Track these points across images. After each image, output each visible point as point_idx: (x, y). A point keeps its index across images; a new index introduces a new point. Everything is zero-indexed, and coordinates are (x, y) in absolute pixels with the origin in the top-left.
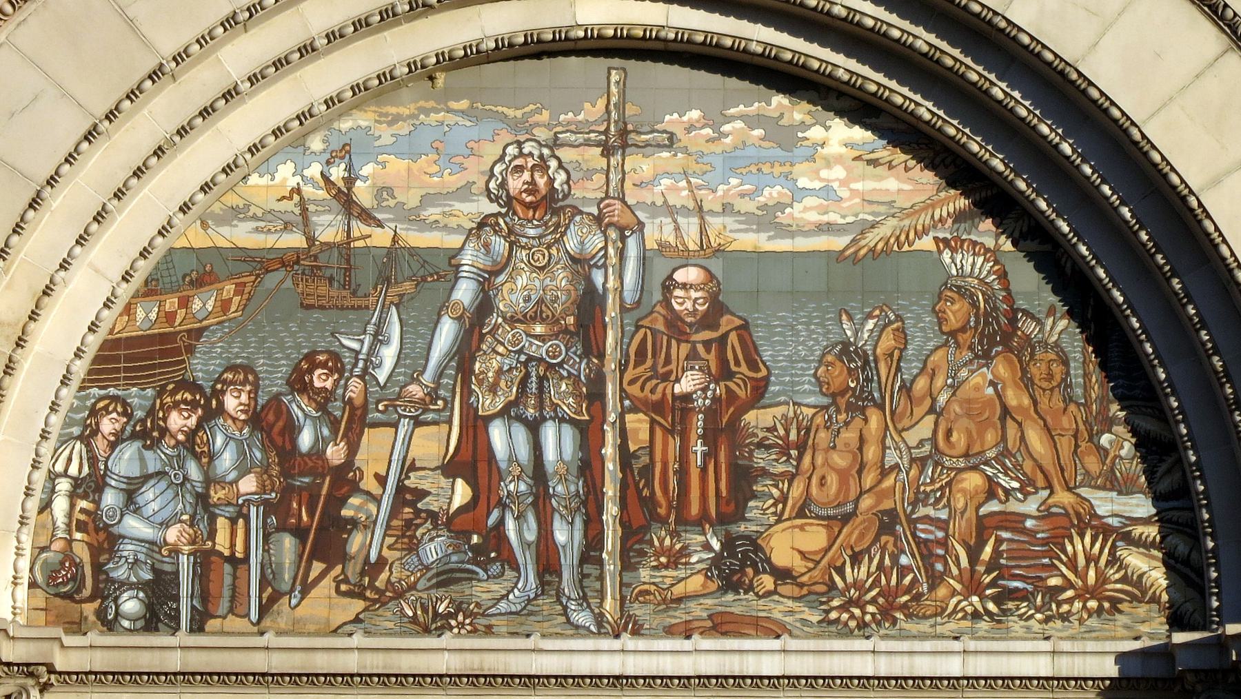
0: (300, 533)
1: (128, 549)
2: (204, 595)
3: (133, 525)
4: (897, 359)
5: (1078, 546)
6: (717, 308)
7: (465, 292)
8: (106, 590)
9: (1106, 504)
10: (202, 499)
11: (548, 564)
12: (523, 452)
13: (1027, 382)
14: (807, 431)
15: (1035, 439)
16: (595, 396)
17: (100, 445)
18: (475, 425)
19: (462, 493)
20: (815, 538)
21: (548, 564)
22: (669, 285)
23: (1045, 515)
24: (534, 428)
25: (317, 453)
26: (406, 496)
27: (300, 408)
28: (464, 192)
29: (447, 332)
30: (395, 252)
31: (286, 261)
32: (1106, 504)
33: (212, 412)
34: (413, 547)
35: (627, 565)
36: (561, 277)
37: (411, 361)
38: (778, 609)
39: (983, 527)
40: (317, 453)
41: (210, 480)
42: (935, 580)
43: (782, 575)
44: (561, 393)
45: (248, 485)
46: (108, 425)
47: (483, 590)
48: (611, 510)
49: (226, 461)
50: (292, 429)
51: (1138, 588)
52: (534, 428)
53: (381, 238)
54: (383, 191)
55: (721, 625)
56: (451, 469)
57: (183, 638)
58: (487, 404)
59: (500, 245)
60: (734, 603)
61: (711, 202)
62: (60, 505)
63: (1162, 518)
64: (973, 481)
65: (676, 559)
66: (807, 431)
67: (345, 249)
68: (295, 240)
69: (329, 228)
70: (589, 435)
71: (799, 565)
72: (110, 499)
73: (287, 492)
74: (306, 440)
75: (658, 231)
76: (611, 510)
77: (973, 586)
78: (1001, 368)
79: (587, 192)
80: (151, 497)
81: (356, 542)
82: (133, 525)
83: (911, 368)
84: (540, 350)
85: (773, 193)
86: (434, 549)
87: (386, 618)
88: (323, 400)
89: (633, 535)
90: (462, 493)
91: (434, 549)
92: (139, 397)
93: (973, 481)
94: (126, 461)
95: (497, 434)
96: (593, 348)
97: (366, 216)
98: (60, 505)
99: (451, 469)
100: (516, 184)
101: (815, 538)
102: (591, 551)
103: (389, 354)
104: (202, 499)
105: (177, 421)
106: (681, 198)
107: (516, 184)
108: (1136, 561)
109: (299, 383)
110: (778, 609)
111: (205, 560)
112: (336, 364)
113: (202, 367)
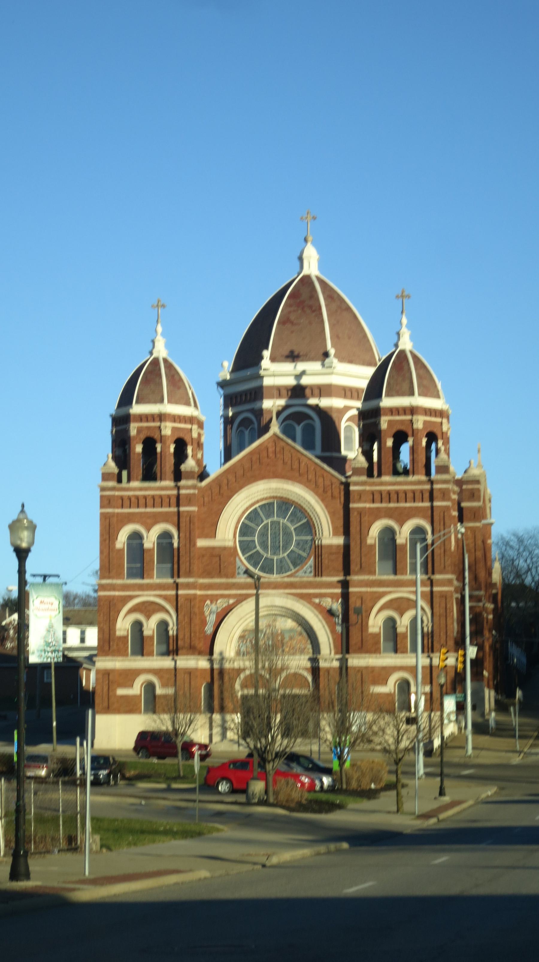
6: (281, 633)
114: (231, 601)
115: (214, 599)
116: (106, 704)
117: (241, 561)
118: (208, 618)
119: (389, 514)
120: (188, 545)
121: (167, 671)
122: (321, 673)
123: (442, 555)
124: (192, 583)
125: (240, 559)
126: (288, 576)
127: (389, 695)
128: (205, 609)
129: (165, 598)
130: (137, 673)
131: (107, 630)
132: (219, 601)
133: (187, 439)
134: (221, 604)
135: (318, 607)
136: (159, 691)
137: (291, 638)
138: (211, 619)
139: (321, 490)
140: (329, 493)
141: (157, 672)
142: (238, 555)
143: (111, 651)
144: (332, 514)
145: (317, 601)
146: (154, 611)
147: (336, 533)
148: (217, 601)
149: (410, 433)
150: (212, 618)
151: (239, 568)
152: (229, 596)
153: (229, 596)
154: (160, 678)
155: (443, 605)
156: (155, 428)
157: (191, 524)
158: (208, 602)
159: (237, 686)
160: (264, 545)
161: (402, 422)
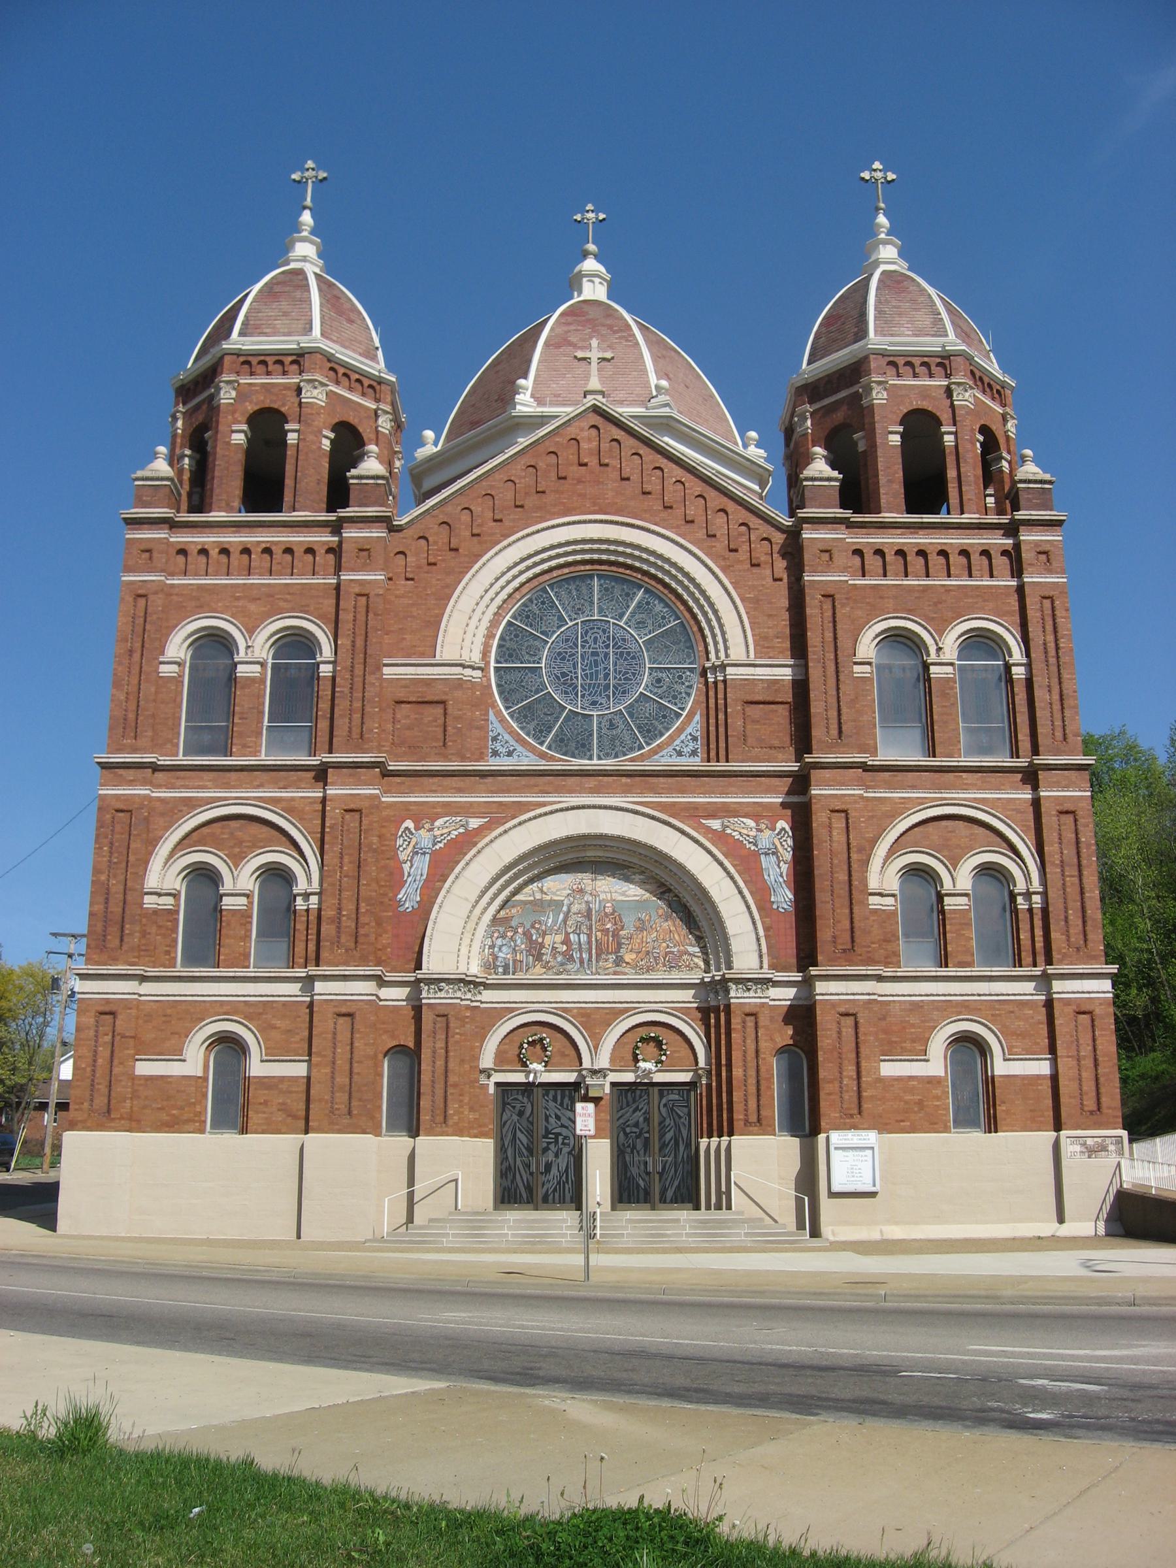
0: (533, 956)
1: (500, 959)
2: (515, 968)
3: (500, 954)
4: (649, 921)
5: (685, 957)
6: (614, 911)
7: (565, 909)
8: (496, 967)
9: (690, 949)
10: (514, 949)
11: (582, 961)
12: (577, 940)
13: (675, 925)
14: (632, 935)
15: (676, 936)
16: (590, 928)
17: (494, 939)
18: (567, 934)
19: (565, 948)
20: (634, 956)
21: (582, 961)
22: (605, 907)
23: (678, 951)
24: (579, 935)
25: (536, 940)
26: (554, 948)
27: (533, 931)
28: (565, 889)
29: (562, 916)
30: (551, 900)
31: (530, 902)
32: (690, 949)
33: (516, 932)
34: (555, 958)
35: (597, 962)
36: (584, 905)
37: (555, 922)
38: (626, 970)
39: (667, 954)
40: (536, 940)
41: (516, 946)
42: (657, 964)
43: (627, 963)
44: (584, 929)
45: (523, 946)
46: (496, 935)
47: (569, 967)
48: (594, 951)
49: (519, 942)
50: (532, 935)
51: (697, 966)
52: (579, 935)
53: (548, 898)
54: (549, 889)
55: (615, 973)
56: (562, 943)
57: (511, 976)
58: (570, 930)
59: (572, 899)
60: (618, 969)
61: (613, 890)
62: (486, 950)
63: (701, 952)
64: (664, 945)
65: (606, 960)
66: (632, 935)
67: (541, 900)
68: (532, 898)
69: (538, 896)
70: (589, 936)
71: (630, 961)
72: (496, 949)
73: (531, 948)
74: (534, 938)
75: (602, 896)
76: (594, 951)
77: (664, 965)
78: (669, 923)
79: (589, 889)
80: (504, 949)
81: (544, 958)
82: (500, 954)
83: (652, 923)
84: (579, 919)
85: (624, 889)
86: (559, 959)
87: (550, 972)
88: (538, 930)
89: (598, 956)
90: (565, 948)
91: (559, 959)
92: (501, 929)
93: (664, 945)
94: (499, 942)
95: (571, 936)
96: (590, 919)
97: (546, 894)
98: (486, 950)
99: (562, 943)
100: (575, 887)
101: (634, 956)
102: (590, 960)
103: (550, 921)
104: (514, 949)
105: (510, 934)
106: (607, 890)
107: (575, 887)
108: (696, 960)
109: (533, 927)
110: (626, 970)
111: (515, 961)
112: (540, 923)
113: (513, 924)
114: (474, 823)
115: (424, 815)
116: (100, 1101)
117: (502, 721)
118: (406, 867)
119: (906, 602)
120: (359, 670)
121: (287, 1007)
122: (736, 1022)
123: (1057, 707)
124: (434, 624)
125: (498, 714)
126: (632, 760)
127: (932, 1081)
128: (400, 842)
129: (290, 808)
130: (196, 1012)
131: (116, 888)
132: (438, 823)
133: (365, 431)
134: (446, 828)
135: (720, 838)
136: (257, 1067)
137: (641, 927)
138: (417, 869)
139: (720, 545)
140: (743, 555)
141: (253, 1012)
142: (494, 705)
143: (125, 947)
144: (754, 604)
145: (716, 824)
146: (257, 845)
147: (763, 646)
148: (433, 821)
149: (945, 416)
150: (417, 868)
151: (495, 739)
152: (467, 810)
153: (467, 810)
154: (265, 1029)
155: (1069, 836)
156: (286, 387)
157: (371, 615)
158: (409, 824)
159: (487, 1060)
160: (565, 681)
161: (924, 392)
